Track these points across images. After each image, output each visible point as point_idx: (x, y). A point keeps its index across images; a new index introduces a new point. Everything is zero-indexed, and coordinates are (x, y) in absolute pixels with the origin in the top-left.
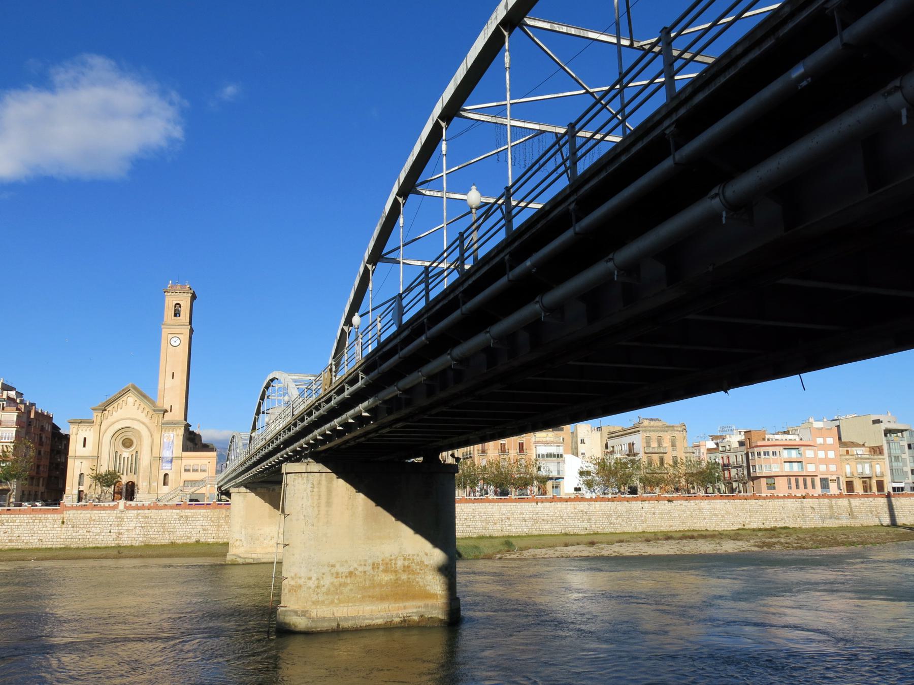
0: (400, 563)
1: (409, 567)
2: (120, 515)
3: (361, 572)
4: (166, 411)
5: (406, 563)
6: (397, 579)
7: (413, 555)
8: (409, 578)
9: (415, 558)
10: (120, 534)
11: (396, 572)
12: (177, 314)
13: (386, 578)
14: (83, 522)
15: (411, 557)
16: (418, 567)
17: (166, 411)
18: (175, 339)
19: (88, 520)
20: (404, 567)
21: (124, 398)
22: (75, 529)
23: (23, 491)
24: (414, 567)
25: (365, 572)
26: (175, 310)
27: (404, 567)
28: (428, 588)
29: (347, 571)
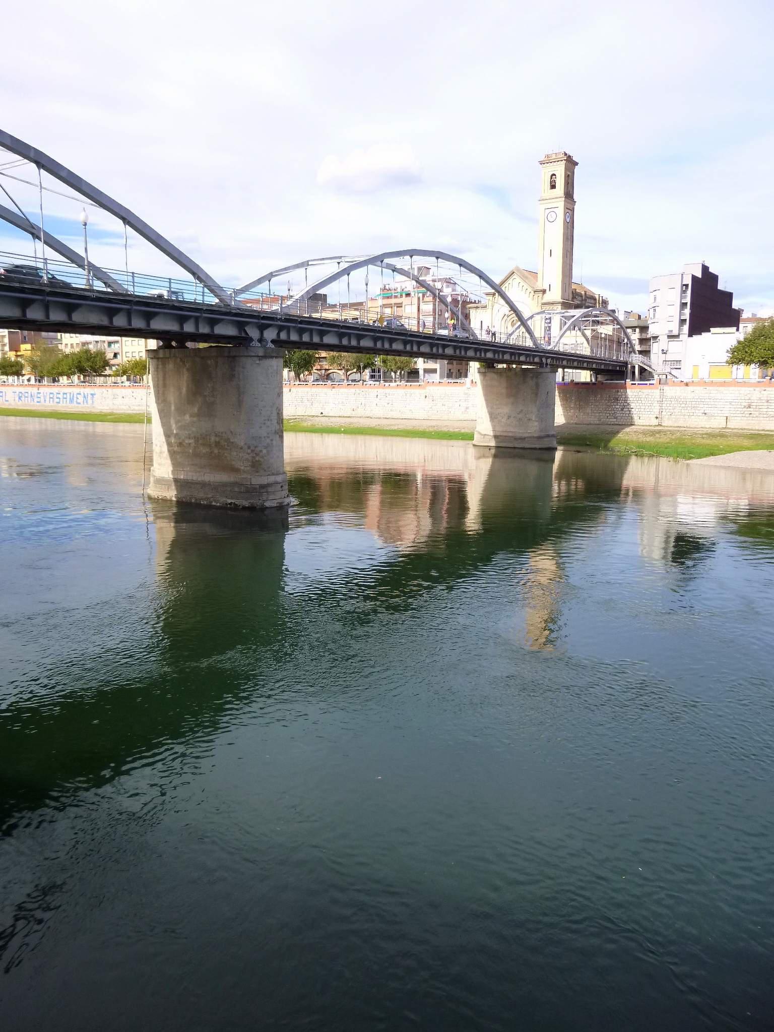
0: (213, 439)
1: (219, 442)
2: (466, 392)
3: (187, 443)
4: (544, 291)
5: (217, 439)
6: (211, 453)
7: (222, 433)
8: (219, 452)
9: (224, 435)
10: (467, 408)
11: (210, 446)
12: (553, 187)
13: (204, 451)
14: (440, 396)
15: (220, 434)
16: (226, 443)
17: (544, 291)
18: (554, 215)
19: (443, 395)
20: (216, 442)
21: (510, 281)
22: (434, 402)
23: (450, 370)
24: (223, 443)
25: (190, 444)
26: (551, 182)
27: (216, 442)
28: (233, 463)
29: (178, 442)
